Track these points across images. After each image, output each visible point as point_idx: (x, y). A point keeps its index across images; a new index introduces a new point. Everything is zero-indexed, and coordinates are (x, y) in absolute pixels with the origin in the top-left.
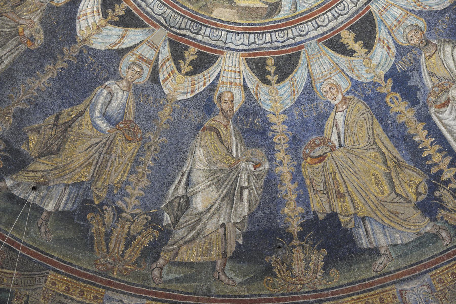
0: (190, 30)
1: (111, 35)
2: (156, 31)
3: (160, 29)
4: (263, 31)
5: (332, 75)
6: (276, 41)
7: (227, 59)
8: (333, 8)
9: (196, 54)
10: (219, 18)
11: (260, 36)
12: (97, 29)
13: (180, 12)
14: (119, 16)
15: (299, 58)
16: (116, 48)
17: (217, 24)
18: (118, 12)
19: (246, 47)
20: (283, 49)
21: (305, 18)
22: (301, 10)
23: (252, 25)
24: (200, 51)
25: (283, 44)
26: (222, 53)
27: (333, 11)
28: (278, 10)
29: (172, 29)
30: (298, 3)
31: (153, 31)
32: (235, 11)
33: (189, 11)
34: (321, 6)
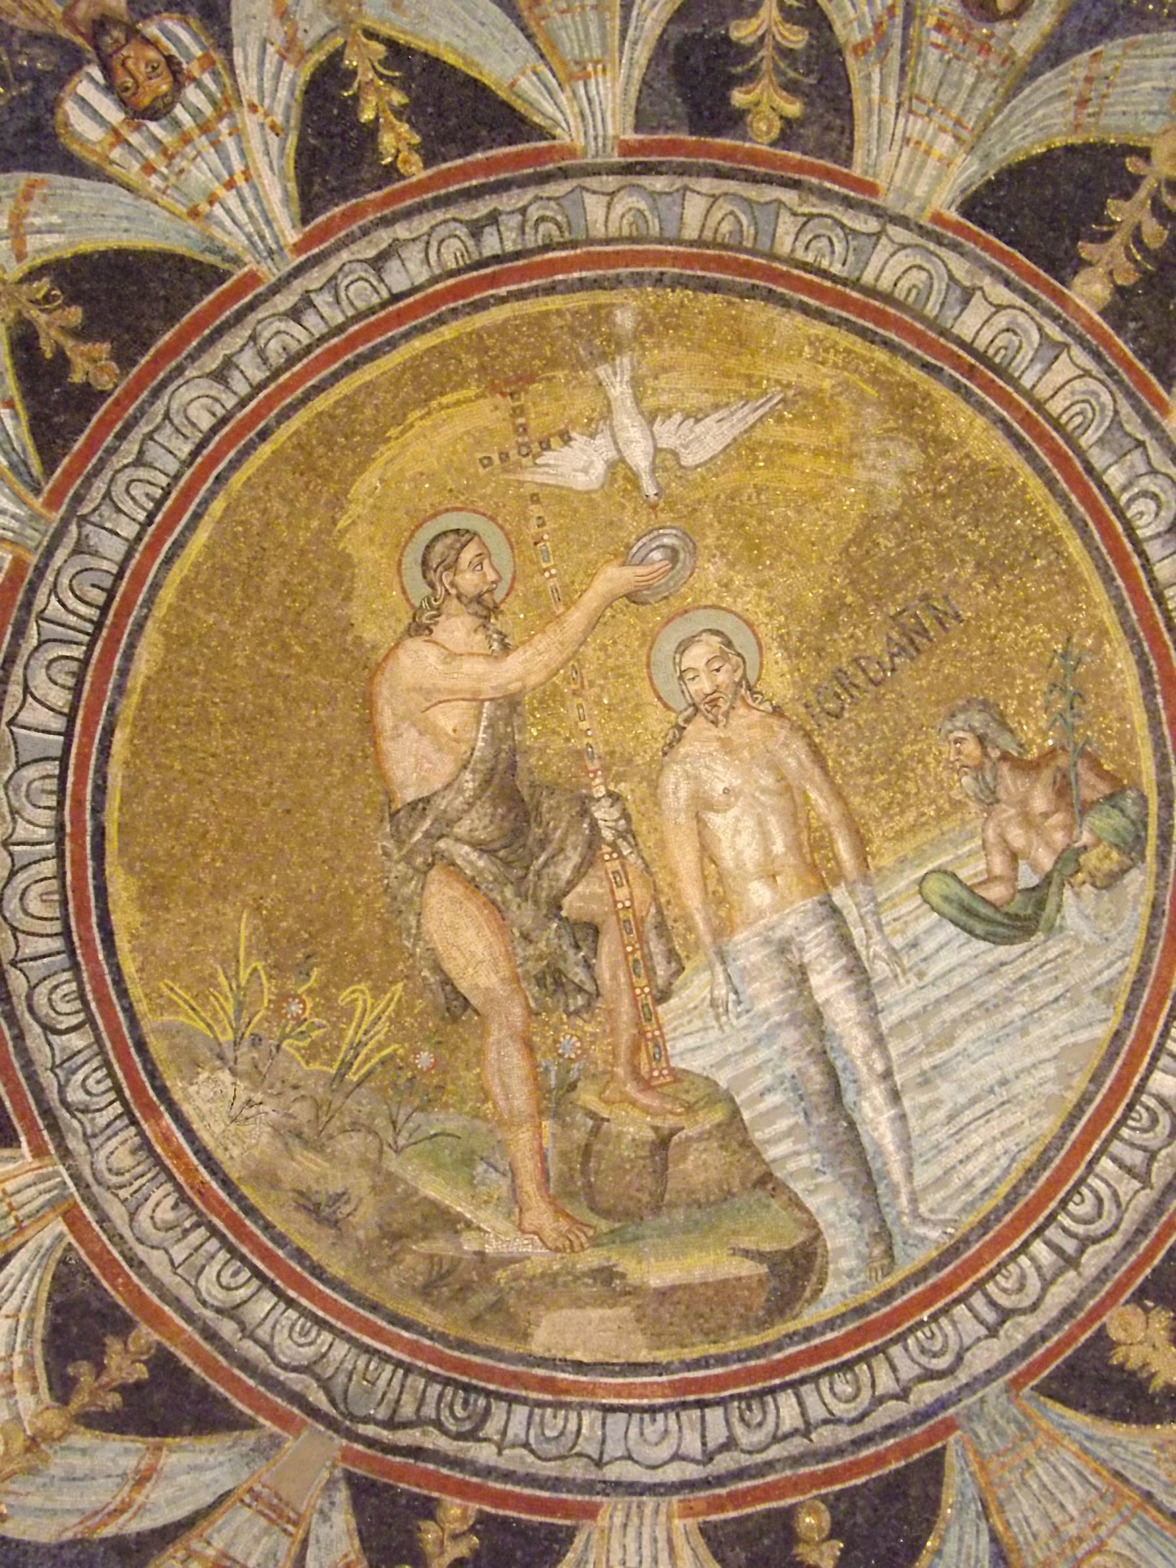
0: (438, 1424)
1: (90, 1477)
2: (290, 1444)
3: (305, 1433)
4: (759, 1386)
5: (1103, 1531)
6: (825, 1422)
7: (616, 1536)
8: (1052, 1218)
9: (472, 1530)
10: (560, 1355)
11: (749, 1408)
12: (28, 1450)
13: (388, 1350)
14: (123, 1389)
15: (939, 1482)
16: (109, 1531)
17: (551, 1385)
18: (120, 1369)
19: (693, 1472)
20: (865, 1453)
21: (937, 1291)
22: (911, 1260)
23: (707, 1366)
24: (488, 1515)
25: (859, 1431)
26: (590, 1512)
27: (1052, 1233)
28: (814, 1278)
29: (362, 1429)
30: (895, 1230)
31: (276, 1443)
32: (625, 1311)
33: (428, 1342)
34: (998, 1220)
